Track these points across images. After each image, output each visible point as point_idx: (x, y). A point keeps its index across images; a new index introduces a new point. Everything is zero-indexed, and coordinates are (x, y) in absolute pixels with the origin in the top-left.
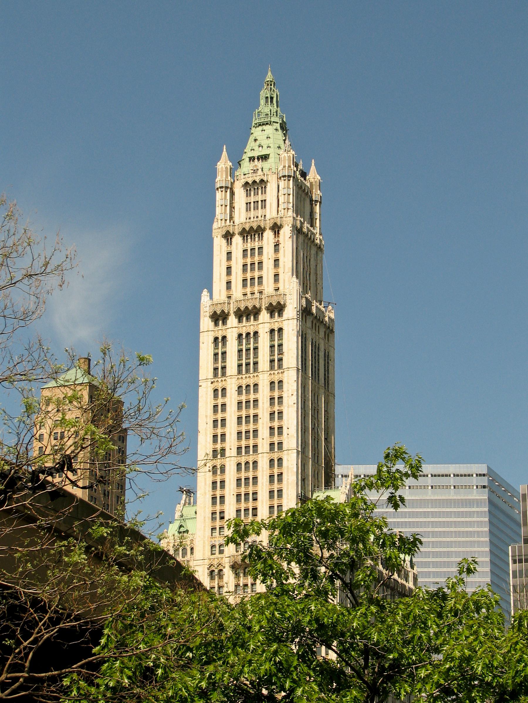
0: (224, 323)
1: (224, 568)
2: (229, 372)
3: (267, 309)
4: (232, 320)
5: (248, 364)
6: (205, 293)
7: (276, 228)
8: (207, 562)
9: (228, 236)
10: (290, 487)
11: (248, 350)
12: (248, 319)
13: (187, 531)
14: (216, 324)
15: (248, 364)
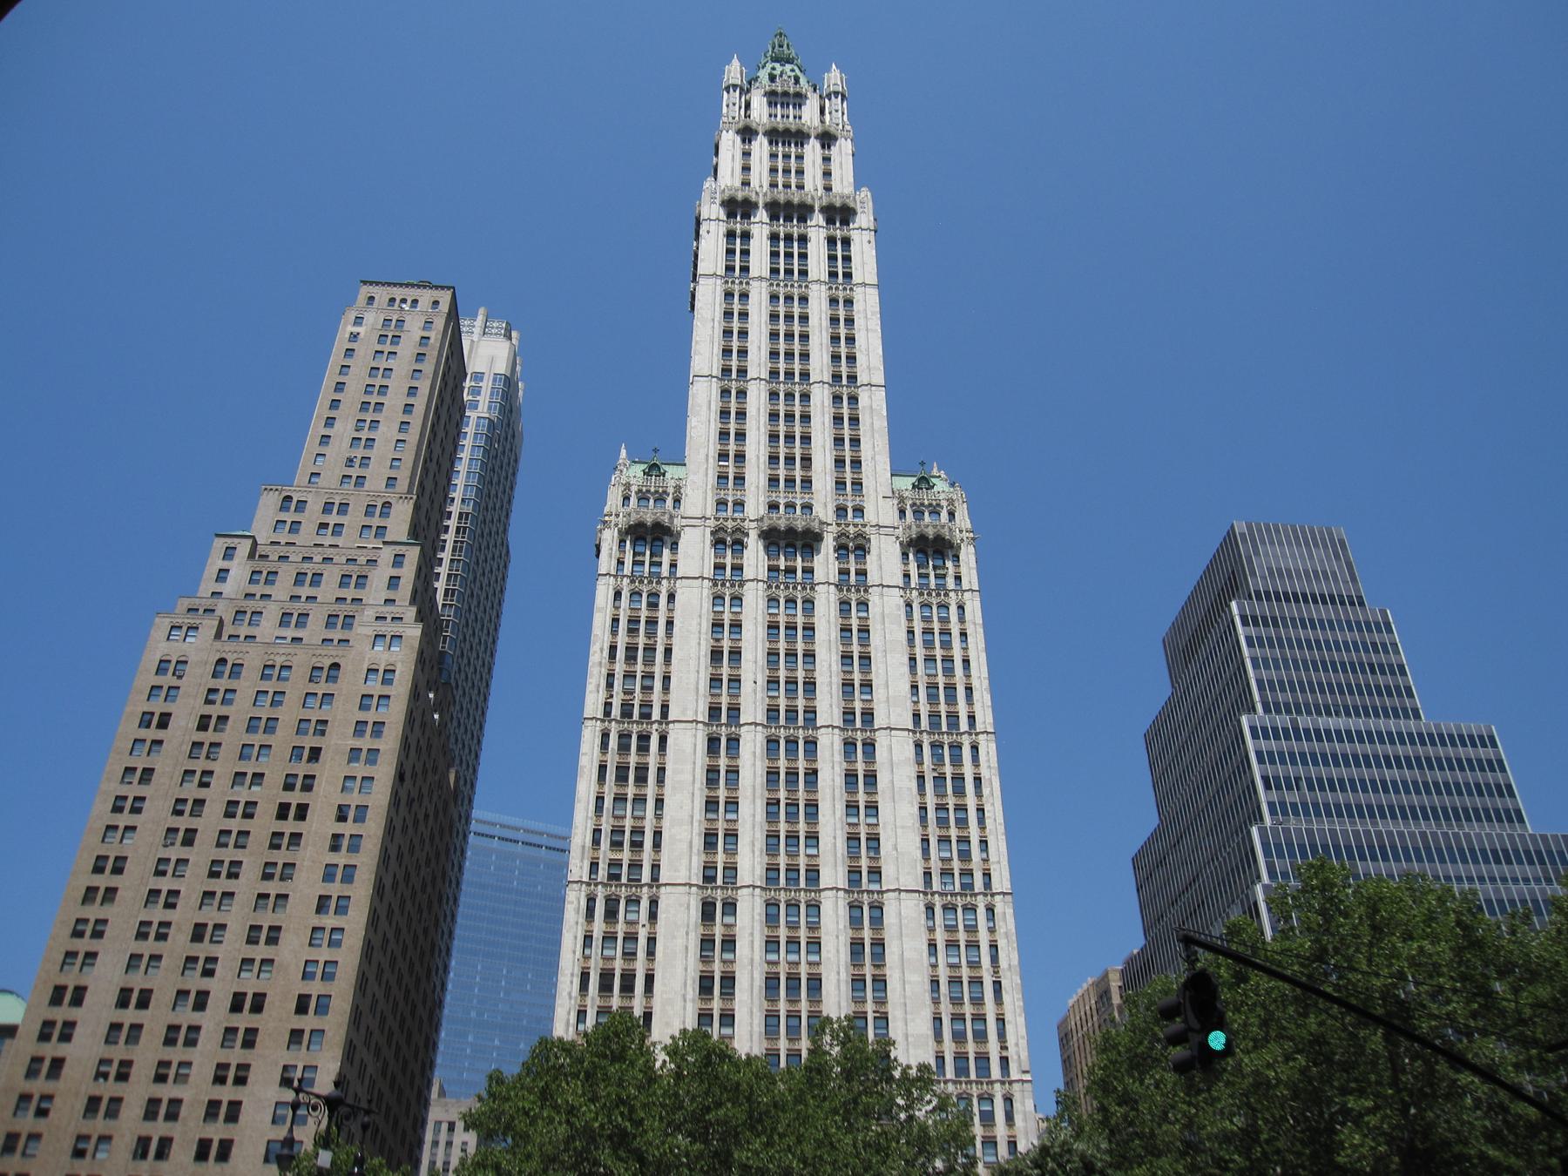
0: (746, 216)
1: (747, 535)
2: (754, 272)
3: (824, 210)
4: (762, 215)
5: (789, 272)
6: (709, 183)
7: (827, 139)
8: (712, 523)
9: (747, 134)
10: (876, 435)
11: (789, 255)
12: (788, 219)
13: (664, 475)
14: (731, 215)
15: (789, 272)
